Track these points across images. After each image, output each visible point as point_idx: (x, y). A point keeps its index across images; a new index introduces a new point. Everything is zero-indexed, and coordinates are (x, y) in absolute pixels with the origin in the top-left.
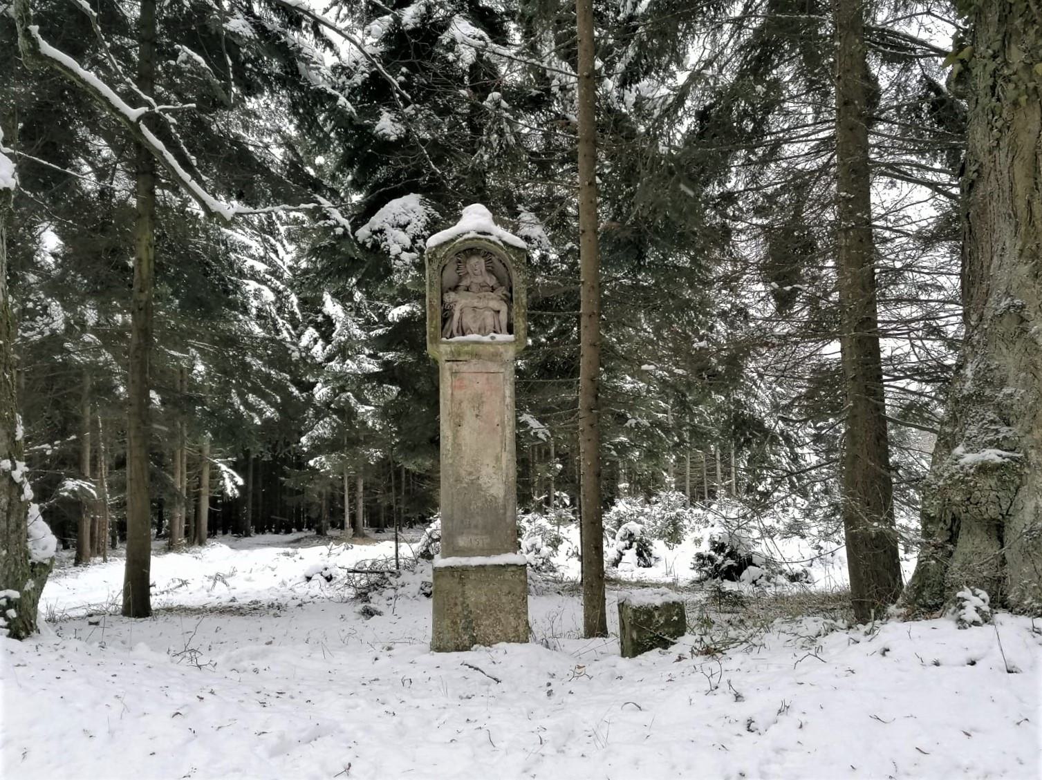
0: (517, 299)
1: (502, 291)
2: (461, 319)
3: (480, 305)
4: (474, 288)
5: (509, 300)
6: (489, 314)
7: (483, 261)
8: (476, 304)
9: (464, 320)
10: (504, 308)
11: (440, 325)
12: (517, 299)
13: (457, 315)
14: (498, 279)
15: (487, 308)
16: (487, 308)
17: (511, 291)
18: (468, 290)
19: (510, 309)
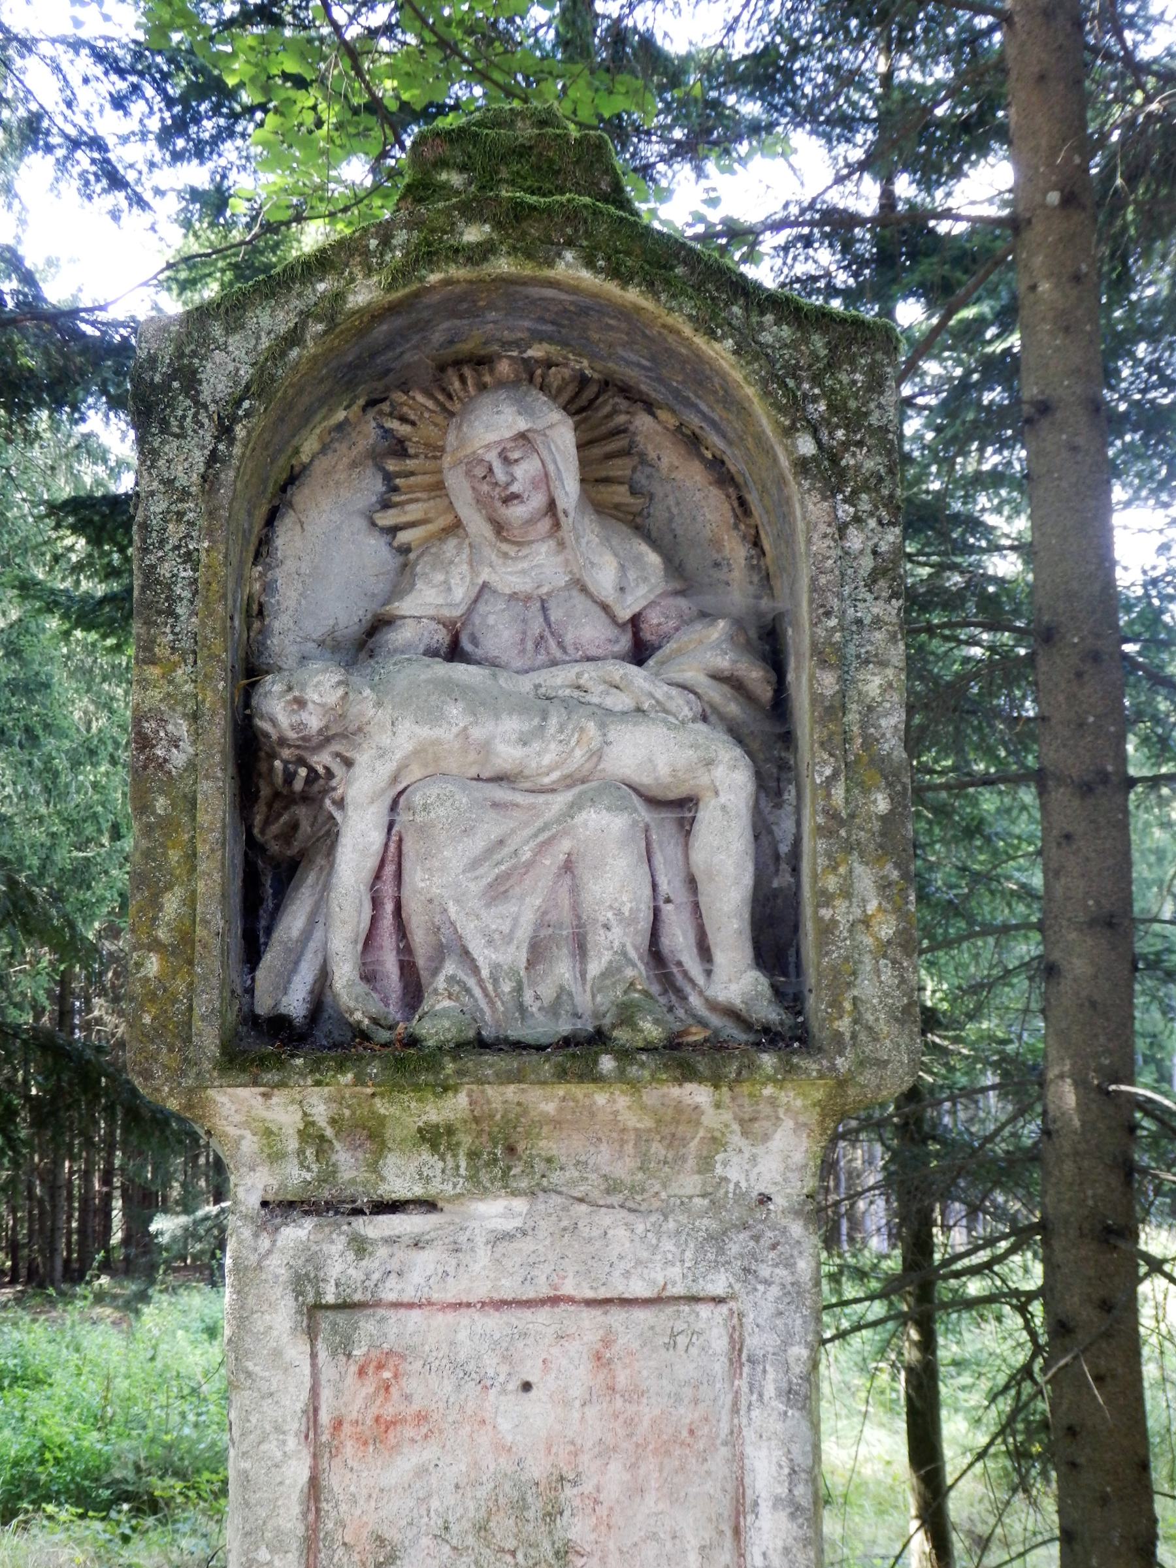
0: (833, 710)
1: (707, 651)
2: (391, 865)
3: (547, 757)
4: (498, 632)
5: (767, 728)
6: (606, 827)
7: (562, 436)
8: (508, 755)
9: (420, 881)
10: (729, 783)
11: (216, 919)
12: (833, 710)
13: (359, 839)
14: (675, 567)
15: (589, 786)
16: (589, 786)
17: (769, 643)
18: (454, 652)
19: (774, 777)
